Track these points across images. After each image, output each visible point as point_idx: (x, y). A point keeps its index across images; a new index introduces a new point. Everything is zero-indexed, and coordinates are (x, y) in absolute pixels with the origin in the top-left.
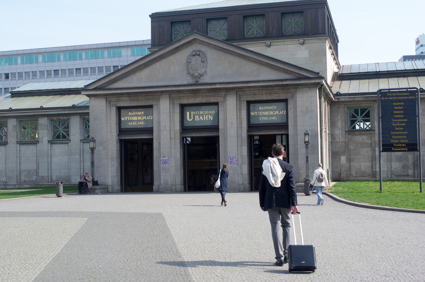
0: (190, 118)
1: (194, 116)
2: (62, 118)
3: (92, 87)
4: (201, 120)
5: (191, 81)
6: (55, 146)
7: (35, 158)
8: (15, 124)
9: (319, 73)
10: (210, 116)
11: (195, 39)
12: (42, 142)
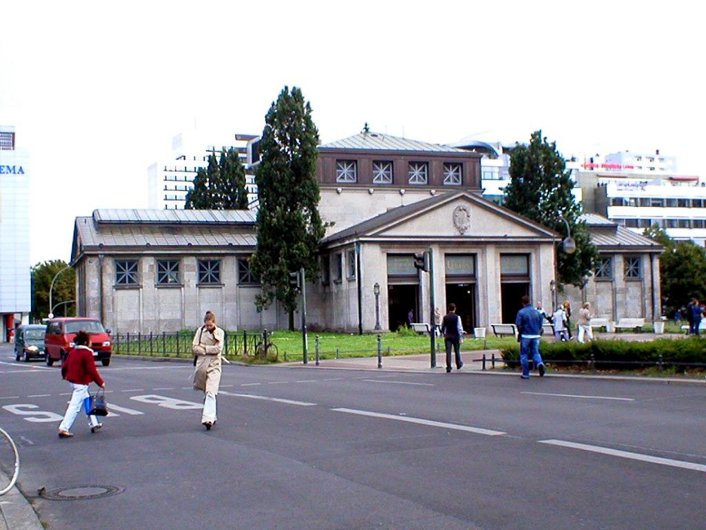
2: (212, 258)
3: (370, 234)
5: (458, 234)
6: (202, 290)
7: (178, 306)
8: (152, 263)
11: (463, 196)
12: (189, 286)
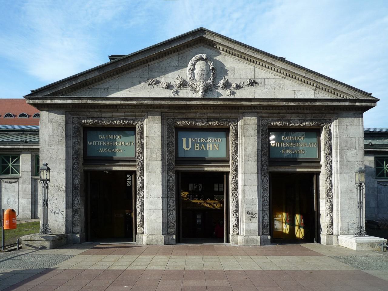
0: (187, 147)
1: (193, 144)
4: (203, 149)
9: (371, 94)
10: (214, 145)
